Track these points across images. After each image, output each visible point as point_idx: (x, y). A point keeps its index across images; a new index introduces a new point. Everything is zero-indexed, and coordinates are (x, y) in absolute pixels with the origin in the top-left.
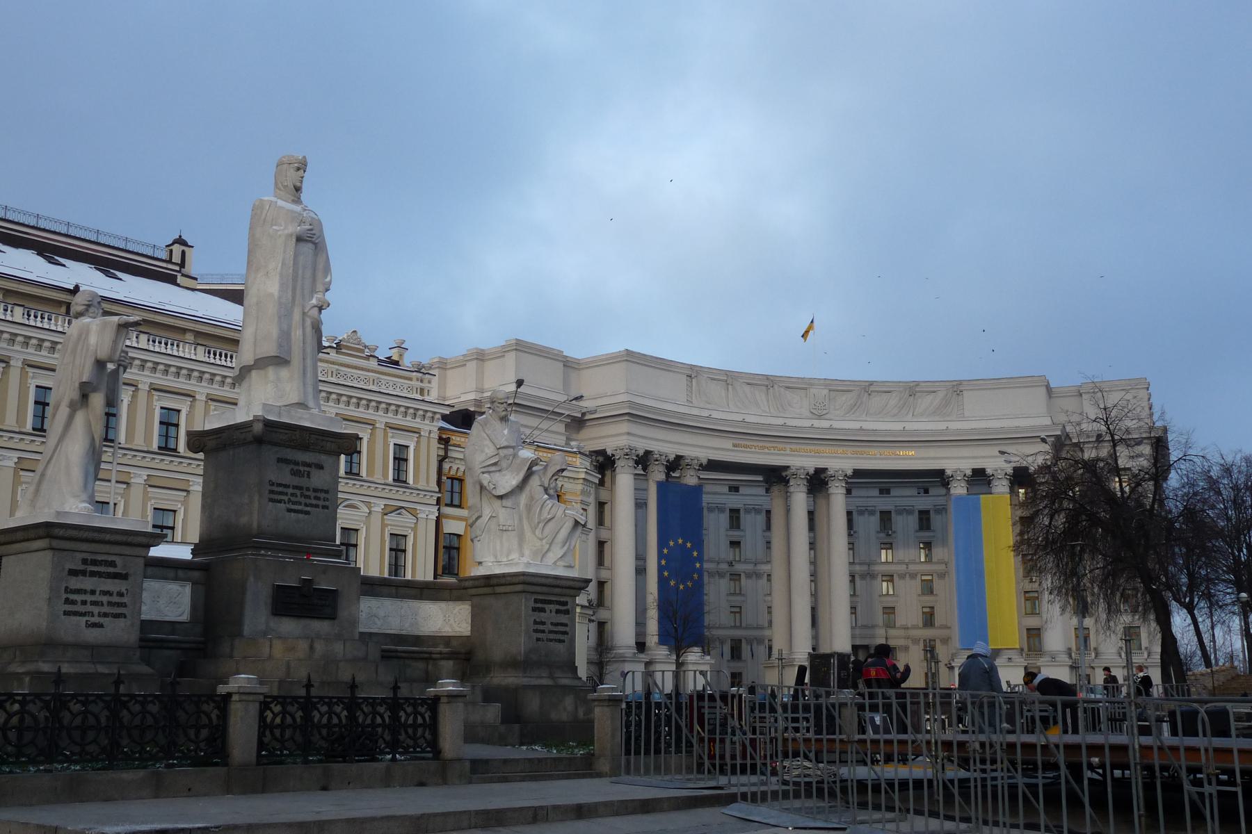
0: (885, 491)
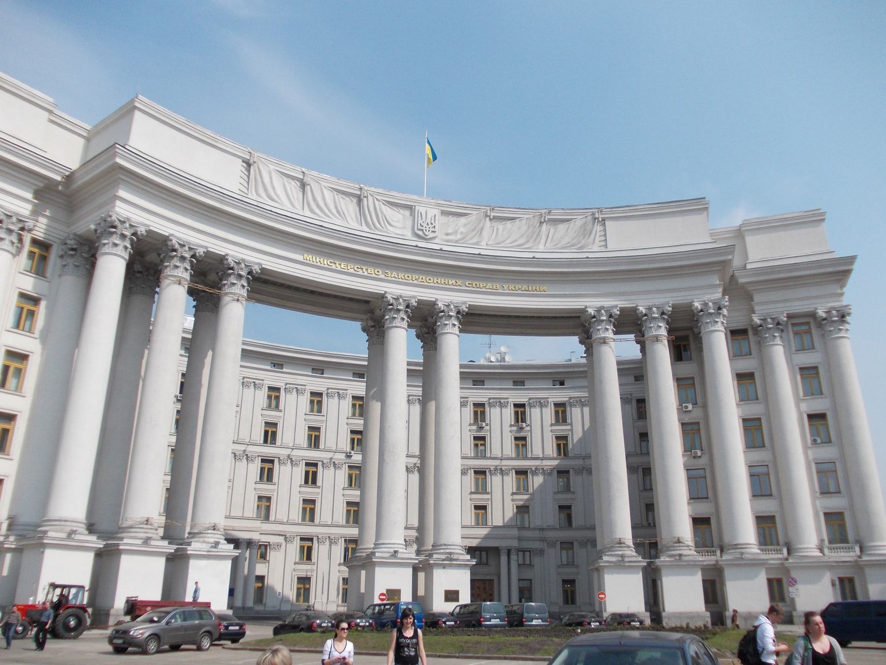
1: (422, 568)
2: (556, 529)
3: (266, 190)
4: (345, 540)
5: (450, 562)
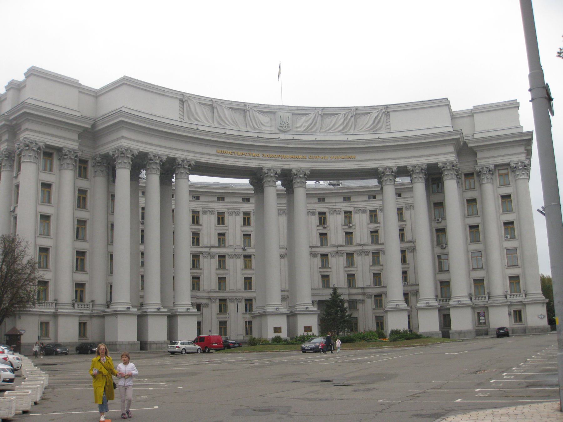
0: (347, 198)
1: (292, 316)
2: (371, 288)
3: (193, 115)
4: (245, 300)
5: (306, 313)
